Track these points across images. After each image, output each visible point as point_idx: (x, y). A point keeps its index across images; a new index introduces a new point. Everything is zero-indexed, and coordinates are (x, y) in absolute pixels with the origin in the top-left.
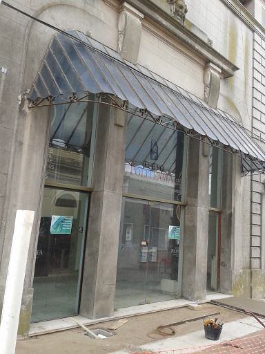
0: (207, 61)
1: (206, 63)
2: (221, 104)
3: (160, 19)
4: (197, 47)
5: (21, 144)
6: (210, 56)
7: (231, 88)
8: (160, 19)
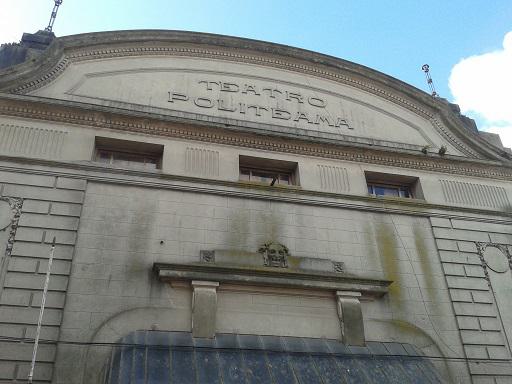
0: (334, 291)
1: (333, 294)
3: (240, 277)
4: (306, 283)
6: (333, 285)
7: (401, 305)
8: (240, 277)
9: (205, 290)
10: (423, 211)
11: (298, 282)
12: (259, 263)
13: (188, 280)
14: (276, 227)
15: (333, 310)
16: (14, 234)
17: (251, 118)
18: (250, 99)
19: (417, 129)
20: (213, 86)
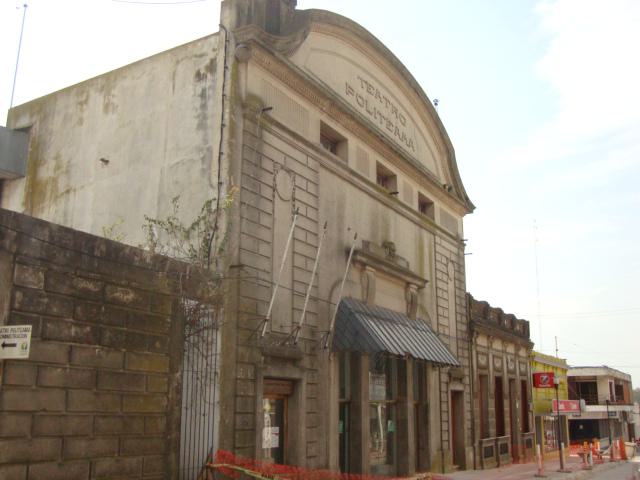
0: (408, 284)
2: (418, 315)
5: (330, 379)
6: (409, 279)
10: (433, 229)
12: (383, 254)
13: (364, 265)
14: (386, 229)
15: (403, 295)
17: (376, 122)
19: (435, 159)
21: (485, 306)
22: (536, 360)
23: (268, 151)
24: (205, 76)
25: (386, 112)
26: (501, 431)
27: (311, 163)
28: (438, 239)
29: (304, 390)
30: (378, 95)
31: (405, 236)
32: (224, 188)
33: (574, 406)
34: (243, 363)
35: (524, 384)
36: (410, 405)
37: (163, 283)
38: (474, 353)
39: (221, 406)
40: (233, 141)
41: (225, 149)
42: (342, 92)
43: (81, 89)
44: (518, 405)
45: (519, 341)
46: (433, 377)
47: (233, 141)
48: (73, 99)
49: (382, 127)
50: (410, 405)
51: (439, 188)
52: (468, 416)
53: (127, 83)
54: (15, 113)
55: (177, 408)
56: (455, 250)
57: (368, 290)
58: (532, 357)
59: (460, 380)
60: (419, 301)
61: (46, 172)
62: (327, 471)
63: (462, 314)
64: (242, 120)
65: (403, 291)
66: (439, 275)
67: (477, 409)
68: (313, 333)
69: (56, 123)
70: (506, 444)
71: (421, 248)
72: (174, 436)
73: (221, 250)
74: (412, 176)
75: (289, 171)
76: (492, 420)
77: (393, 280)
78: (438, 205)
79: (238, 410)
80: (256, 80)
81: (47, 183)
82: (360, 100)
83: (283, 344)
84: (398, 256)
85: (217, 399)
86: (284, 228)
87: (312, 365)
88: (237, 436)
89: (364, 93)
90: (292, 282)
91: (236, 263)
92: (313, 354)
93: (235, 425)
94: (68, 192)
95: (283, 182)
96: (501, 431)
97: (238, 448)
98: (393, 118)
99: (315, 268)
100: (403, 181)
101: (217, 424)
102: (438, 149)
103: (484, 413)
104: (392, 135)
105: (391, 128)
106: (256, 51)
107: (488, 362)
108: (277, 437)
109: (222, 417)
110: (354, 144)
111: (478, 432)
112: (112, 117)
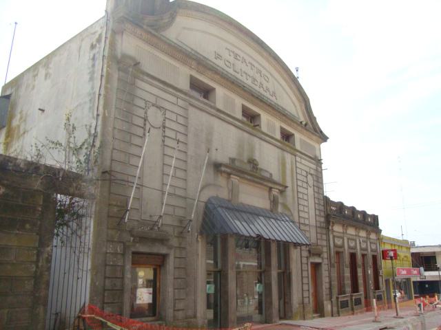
2: (280, 209)
5: (198, 255)
6: (270, 185)
9: (234, 179)
10: (294, 152)
11: (262, 182)
12: (248, 168)
13: (229, 174)
14: (252, 150)
15: (267, 197)
16: (164, 131)
18: (244, 68)
19: (296, 107)
20: (231, 54)
21: (340, 206)
22: (384, 241)
23: (139, 93)
24: (96, 45)
25: (251, 73)
26: (355, 289)
27: (181, 103)
28: (298, 159)
29: (171, 263)
30: (244, 61)
31: (269, 158)
32: (100, 118)
33: (415, 272)
34: (113, 241)
35: (374, 258)
36: (274, 273)
37: (37, 184)
38: (331, 236)
39: (91, 273)
40: (109, 86)
41: (103, 92)
42: (212, 58)
43: (35, 68)
44: (370, 272)
45: (369, 228)
46: (295, 254)
47: (109, 86)
48: (31, 74)
49: (249, 82)
50: (274, 273)
51: (297, 124)
52: (325, 280)
53: (56, 59)
54: (5, 87)
55: (47, 273)
56: (314, 167)
57: (233, 191)
58: (380, 239)
59: (319, 255)
60: (280, 200)
61: (15, 123)
62: (195, 320)
63: (319, 210)
64: (117, 71)
65: (266, 194)
66: (300, 183)
67: (334, 275)
68: (181, 221)
69: (22, 91)
70: (360, 299)
71: (283, 165)
72: (42, 294)
73: (96, 161)
74: (269, 113)
75: (159, 108)
76: (348, 282)
77: (259, 186)
78: (298, 137)
79: (107, 275)
80: (130, 45)
81: (15, 128)
82: (227, 63)
83: (151, 229)
84: (261, 170)
85: (89, 267)
86: (150, 146)
87: (180, 244)
88: (106, 294)
89: (231, 59)
90: (164, 182)
91: (108, 169)
92: (181, 235)
93: (104, 285)
94: (24, 133)
95: (155, 117)
96: (355, 289)
97: (106, 303)
98: (257, 76)
99: (171, 172)
100: (265, 118)
101: (88, 286)
102: (298, 98)
103: (341, 278)
104: (257, 88)
105: (256, 83)
106: (129, 26)
107: (356, 244)
108: (151, 296)
109: (92, 280)
110: (221, 92)
111: (335, 291)
112: (49, 81)
